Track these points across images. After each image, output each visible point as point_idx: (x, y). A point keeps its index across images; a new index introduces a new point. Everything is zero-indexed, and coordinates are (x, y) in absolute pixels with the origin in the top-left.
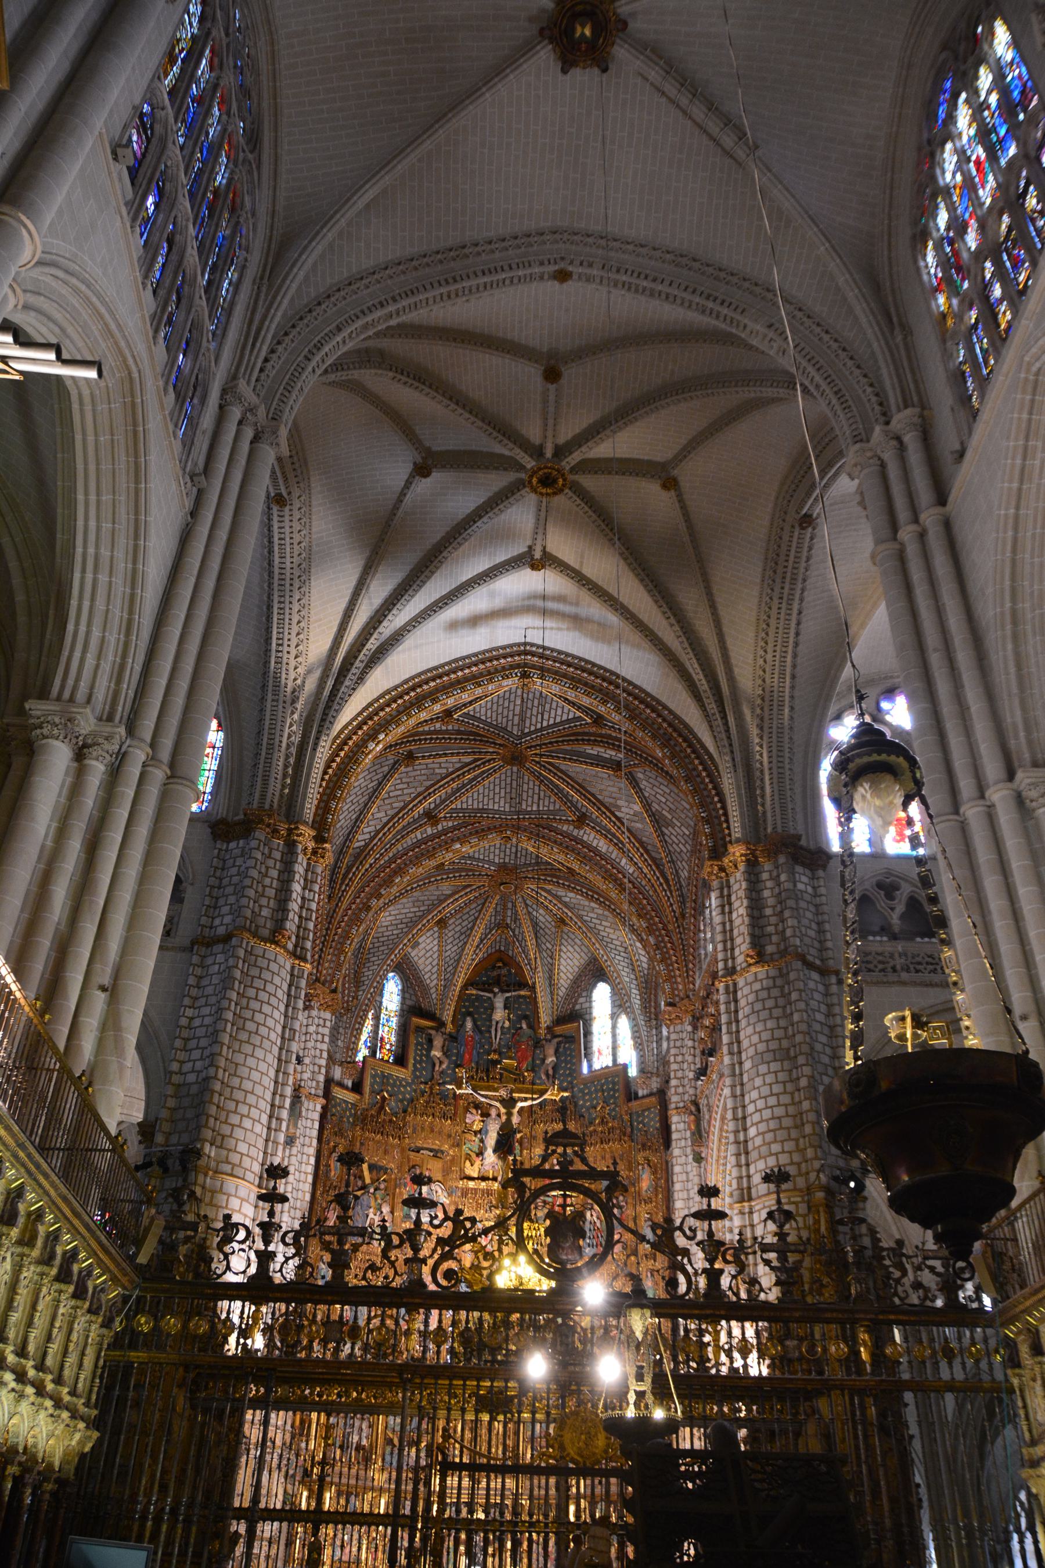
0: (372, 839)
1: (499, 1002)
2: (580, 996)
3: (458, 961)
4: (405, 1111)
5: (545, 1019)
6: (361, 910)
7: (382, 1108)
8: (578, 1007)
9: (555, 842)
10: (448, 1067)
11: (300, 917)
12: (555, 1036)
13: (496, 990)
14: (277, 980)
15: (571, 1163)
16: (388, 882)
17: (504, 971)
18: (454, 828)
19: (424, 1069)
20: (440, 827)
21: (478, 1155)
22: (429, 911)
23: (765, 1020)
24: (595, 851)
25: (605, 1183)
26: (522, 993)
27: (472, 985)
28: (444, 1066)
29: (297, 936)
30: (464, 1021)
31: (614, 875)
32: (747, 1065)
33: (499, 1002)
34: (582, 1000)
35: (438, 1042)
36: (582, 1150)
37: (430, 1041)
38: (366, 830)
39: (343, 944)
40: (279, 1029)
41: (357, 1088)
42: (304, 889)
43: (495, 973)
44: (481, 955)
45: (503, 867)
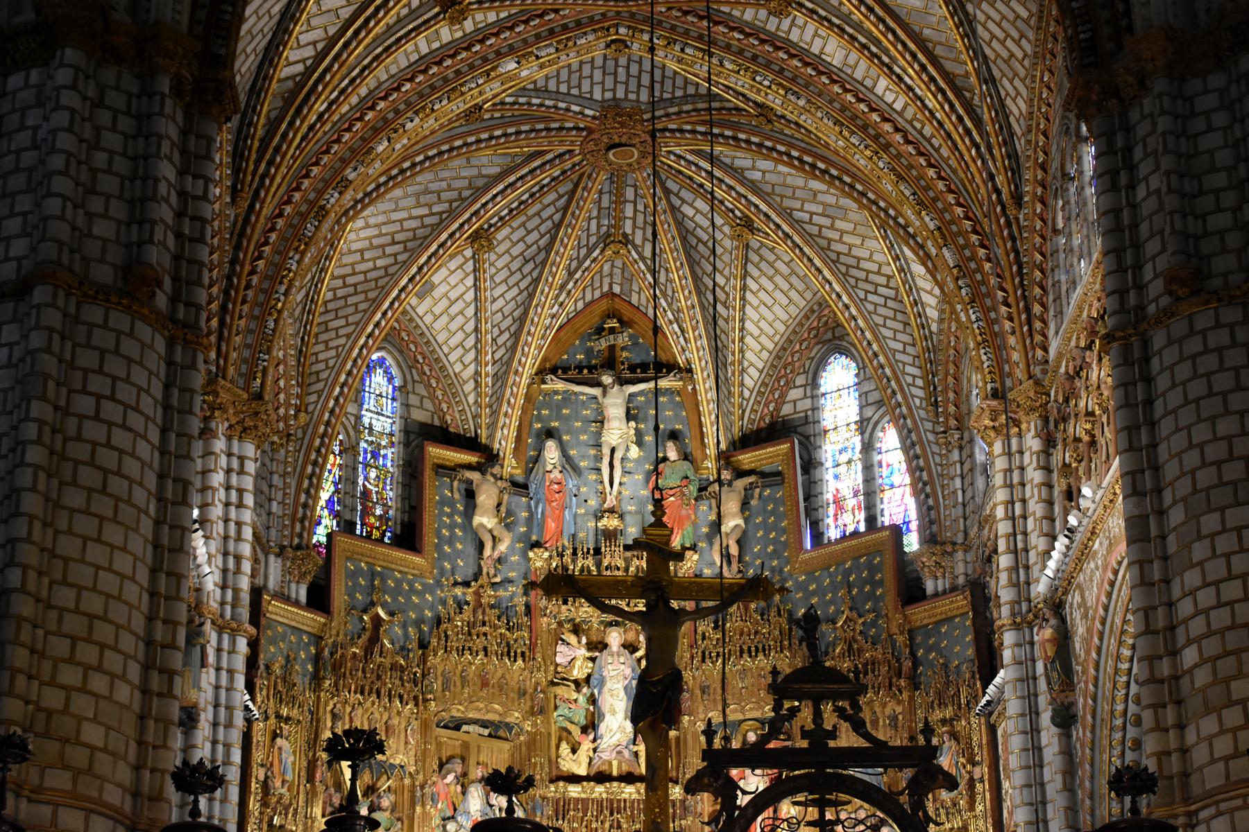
0: (320, 57)
2: (790, 385)
3: (522, 320)
4: (423, 645)
5: (714, 437)
6: (303, 216)
7: (375, 639)
8: (786, 410)
9: (728, 48)
10: (511, 548)
11: (179, 236)
12: (740, 474)
13: (607, 379)
14: (140, 377)
15: (833, 734)
16: (361, 152)
17: (623, 339)
18: (501, 27)
19: (459, 554)
20: (469, 26)
21: (584, 730)
22: (452, 214)
23: (1213, 419)
24: (818, 64)
25: (908, 773)
26: (664, 383)
27: (554, 371)
28: (502, 547)
29: (176, 279)
30: (540, 450)
31: (859, 116)
32: (1176, 516)
33: (615, 404)
34: (794, 394)
35: (487, 496)
36: (856, 707)
37: (470, 495)
38: (304, 38)
39: (269, 293)
40: (151, 481)
41: (319, 599)
42: (181, 173)
43: (603, 344)
44: (570, 307)
45: (612, 109)
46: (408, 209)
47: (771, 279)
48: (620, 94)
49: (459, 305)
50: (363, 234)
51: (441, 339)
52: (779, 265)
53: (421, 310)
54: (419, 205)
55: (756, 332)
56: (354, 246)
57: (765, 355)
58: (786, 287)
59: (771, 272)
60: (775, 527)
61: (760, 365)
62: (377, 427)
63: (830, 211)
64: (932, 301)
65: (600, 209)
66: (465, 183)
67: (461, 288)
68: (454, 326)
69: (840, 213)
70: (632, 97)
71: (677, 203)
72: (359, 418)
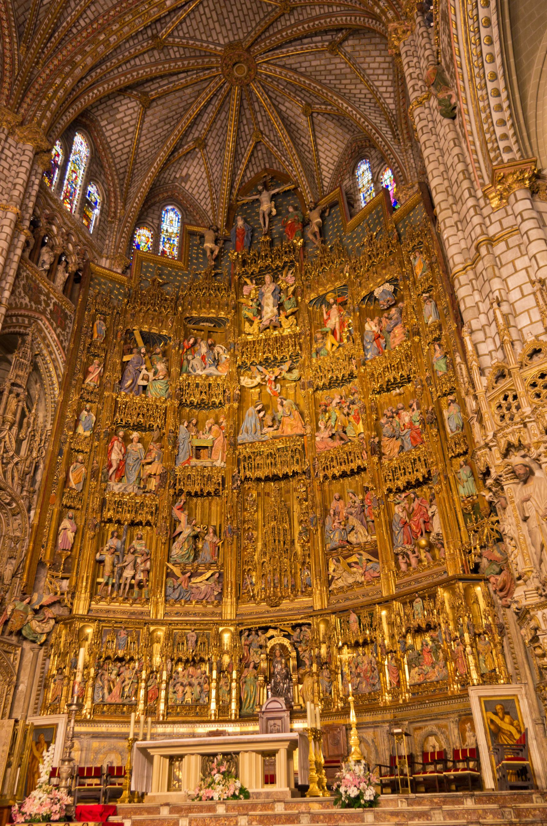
1: (265, 197)
19: (201, 263)
33: (265, 197)
46: (162, 127)
47: (327, 137)
48: (232, 39)
49: (201, 180)
50: (146, 143)
51: (196, 197)
52: (330, 130)
53: (187, 188)
54: (166, 124)
55: (326, 163)
56: (143, 149)
57: (331, 171)
58: (335, 140)
59: (327, 134)
60: (337, 222)
61: (330, 176)
62: (170, 230)
63: (338, 77)
64: (390, 101)
65: (247, 119)
66: (182, 109)
67: (200, 173)
68: (200, 191)
69: (343, 77)
70: (237, 38)
71: (277, 103)
72: (159, 225)
